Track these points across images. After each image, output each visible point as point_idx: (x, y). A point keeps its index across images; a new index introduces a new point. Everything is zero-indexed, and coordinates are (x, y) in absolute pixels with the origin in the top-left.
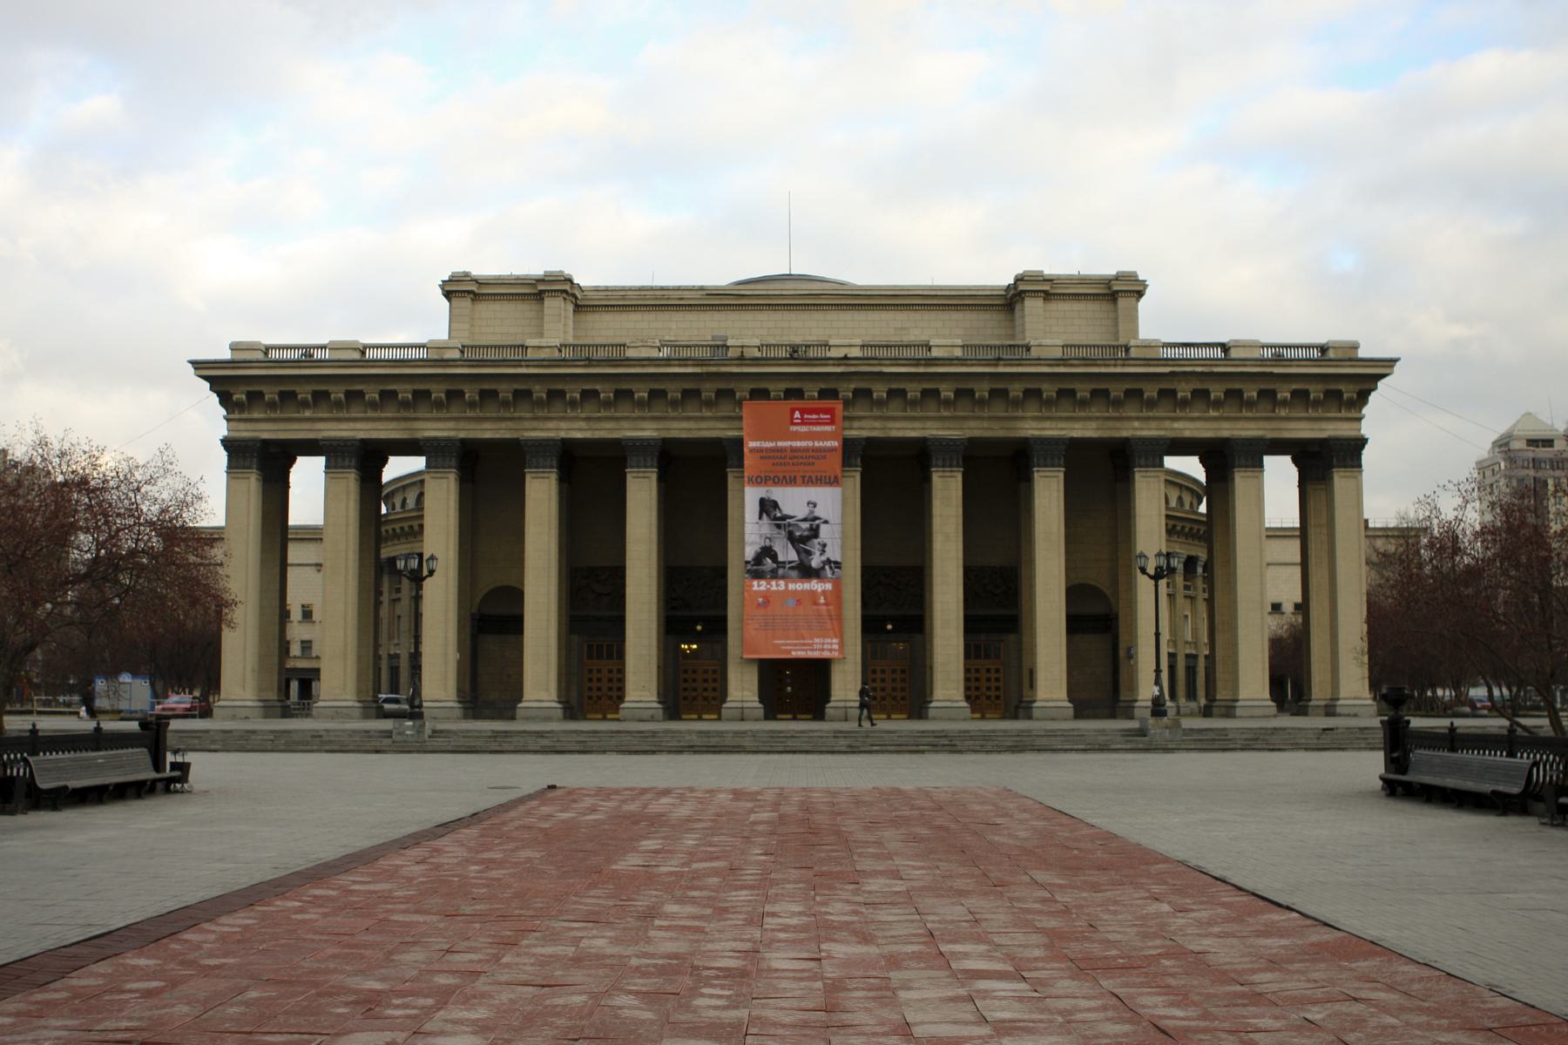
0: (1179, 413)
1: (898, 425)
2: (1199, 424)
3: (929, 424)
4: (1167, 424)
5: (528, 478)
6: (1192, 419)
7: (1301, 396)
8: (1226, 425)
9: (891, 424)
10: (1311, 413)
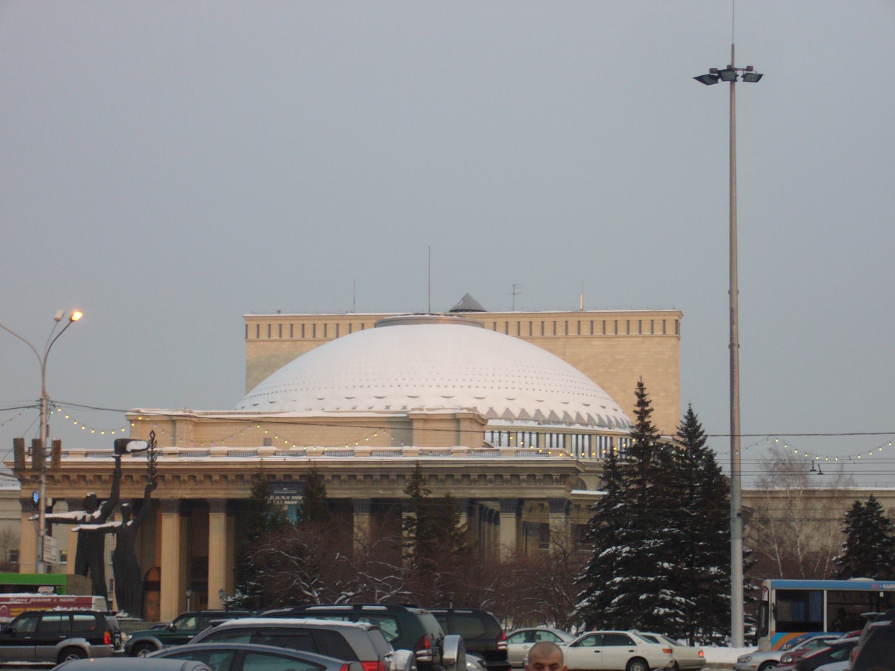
0: (473, 486)
1: (338, 492)
2: (483, 491)
3: (352, 491)
4: (467, 491)
5: (163, 518)
6: (480, 489)
7: (532, 477)
8: (496, 491)
9: (334, 492)
10: (538, 485)
